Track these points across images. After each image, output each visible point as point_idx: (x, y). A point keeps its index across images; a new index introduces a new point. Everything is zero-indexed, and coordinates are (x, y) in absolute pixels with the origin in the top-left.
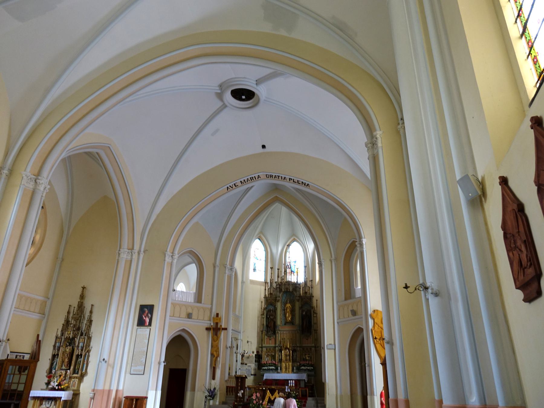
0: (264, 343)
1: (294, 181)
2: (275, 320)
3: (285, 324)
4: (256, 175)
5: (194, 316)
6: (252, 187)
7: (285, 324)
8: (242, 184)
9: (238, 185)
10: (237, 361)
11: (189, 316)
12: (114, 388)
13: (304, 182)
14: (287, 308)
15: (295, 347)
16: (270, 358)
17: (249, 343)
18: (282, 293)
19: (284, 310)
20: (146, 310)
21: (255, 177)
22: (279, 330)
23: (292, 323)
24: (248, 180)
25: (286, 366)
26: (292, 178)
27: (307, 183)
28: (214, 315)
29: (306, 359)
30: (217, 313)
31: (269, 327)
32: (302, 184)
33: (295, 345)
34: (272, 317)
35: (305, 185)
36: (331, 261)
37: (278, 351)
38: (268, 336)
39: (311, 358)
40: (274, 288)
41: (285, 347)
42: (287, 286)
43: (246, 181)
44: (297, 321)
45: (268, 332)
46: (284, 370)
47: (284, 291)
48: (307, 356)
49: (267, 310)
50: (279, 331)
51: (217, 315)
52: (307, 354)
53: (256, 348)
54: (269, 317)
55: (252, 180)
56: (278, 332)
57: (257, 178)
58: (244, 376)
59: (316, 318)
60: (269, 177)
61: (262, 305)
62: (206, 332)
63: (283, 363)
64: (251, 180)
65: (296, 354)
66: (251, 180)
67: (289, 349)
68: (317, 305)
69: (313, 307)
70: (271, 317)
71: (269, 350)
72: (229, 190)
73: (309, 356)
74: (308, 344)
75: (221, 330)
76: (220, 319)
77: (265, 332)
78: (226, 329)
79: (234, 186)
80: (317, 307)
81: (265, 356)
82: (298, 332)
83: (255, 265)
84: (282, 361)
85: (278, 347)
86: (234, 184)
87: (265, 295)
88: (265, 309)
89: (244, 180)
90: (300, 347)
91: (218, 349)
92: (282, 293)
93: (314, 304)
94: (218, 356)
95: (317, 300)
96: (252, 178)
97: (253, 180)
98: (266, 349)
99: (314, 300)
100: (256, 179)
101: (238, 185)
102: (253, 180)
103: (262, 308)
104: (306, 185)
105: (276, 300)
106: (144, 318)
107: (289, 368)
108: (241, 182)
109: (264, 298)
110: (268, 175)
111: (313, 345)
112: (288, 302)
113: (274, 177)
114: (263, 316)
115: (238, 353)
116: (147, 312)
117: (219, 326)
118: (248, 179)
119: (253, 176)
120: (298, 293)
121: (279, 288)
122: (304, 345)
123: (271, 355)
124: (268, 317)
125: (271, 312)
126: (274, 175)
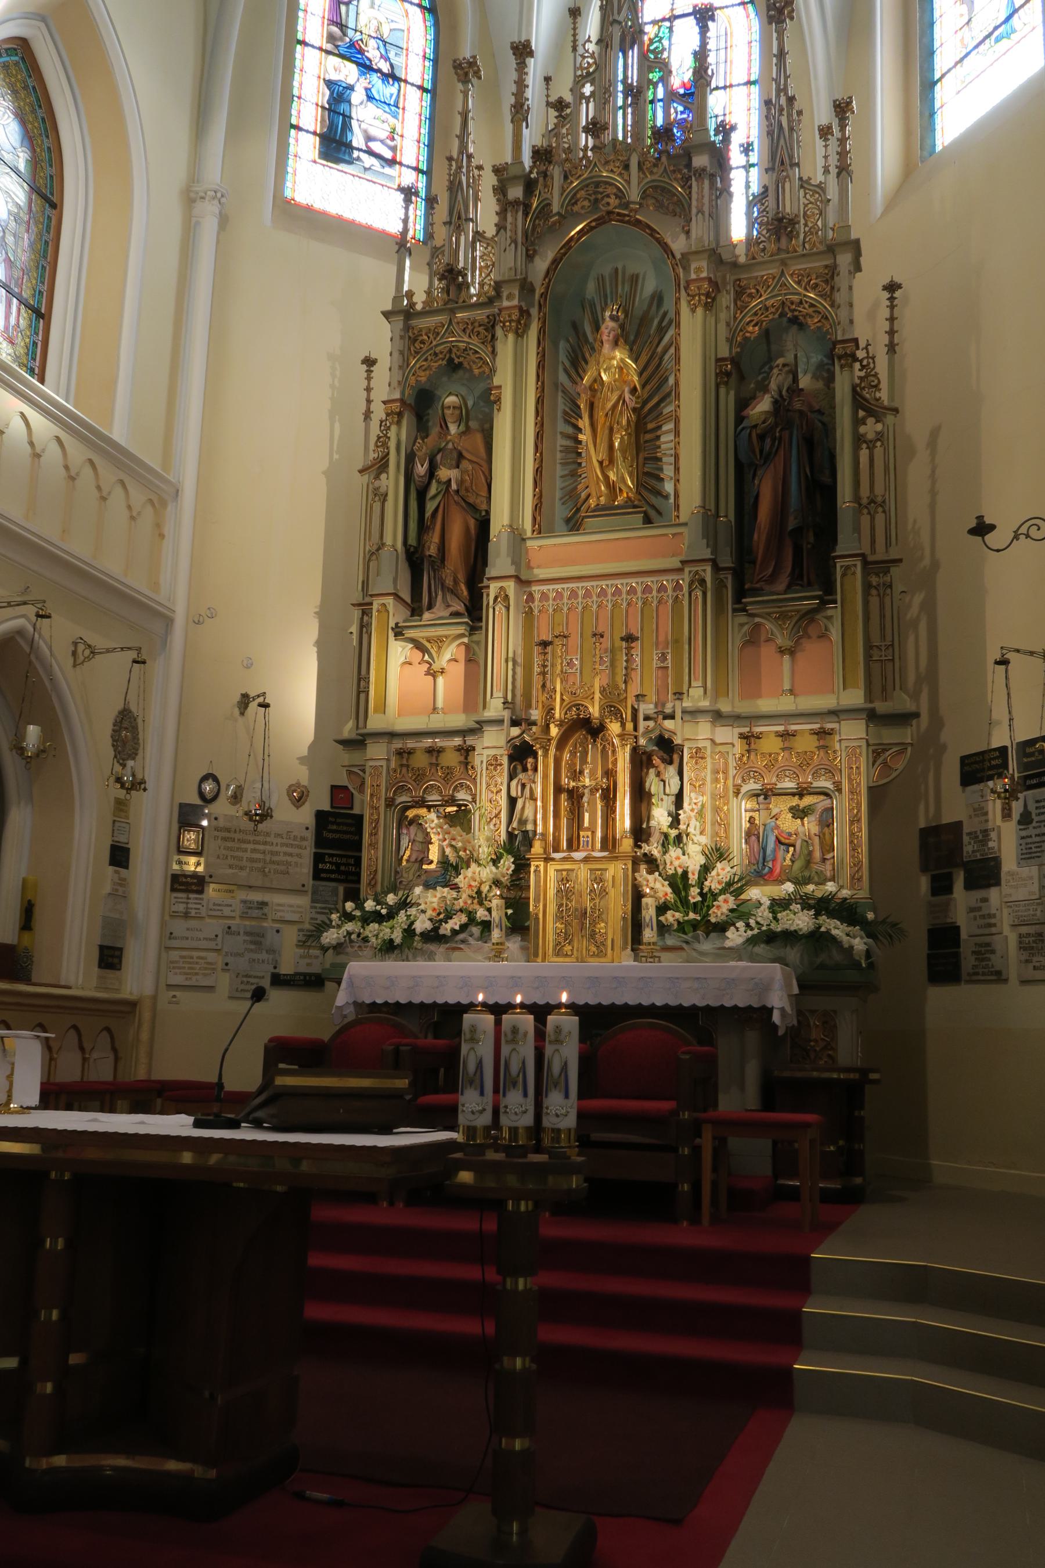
10: (119, 856)
17: (253, 706)
38: (418, 646)
54: (432, 472)
65: (674, 786)
80: (892, 348)
83: (343, 107)
95: (892, 287)
103: (367, 415)
109: (387, 315)
120: (699, 228)
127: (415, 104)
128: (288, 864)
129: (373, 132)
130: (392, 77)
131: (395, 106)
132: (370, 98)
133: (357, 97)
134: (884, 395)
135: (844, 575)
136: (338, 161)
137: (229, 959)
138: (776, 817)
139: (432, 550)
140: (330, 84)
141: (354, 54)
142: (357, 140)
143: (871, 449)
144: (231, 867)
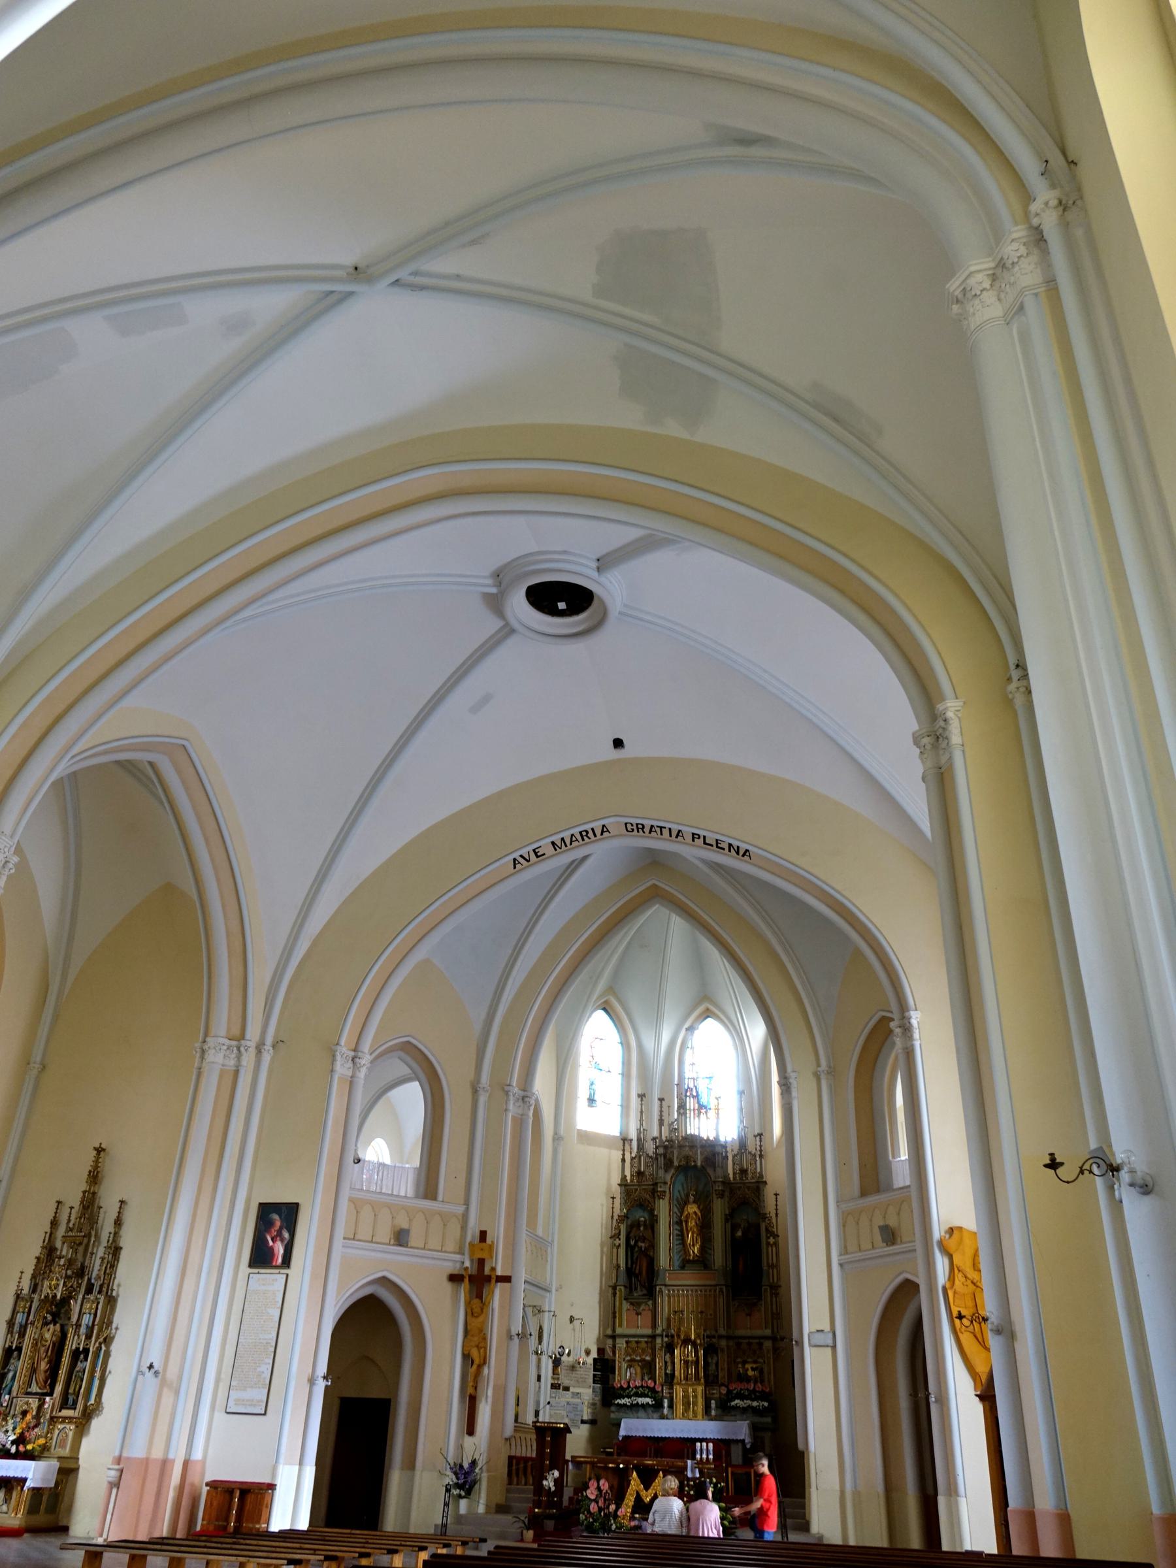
0: (620, 1325)
1: (705, 843)
2: (651, 1254)
3: (682, 1267)
4: (597, 826)
5: (415, 1239)
6: (585, 858)
7: (682, 1267)
8: (556, 850)
9: (544, 854)
10: (539, 1378)
11: (401, 1238)
12: (178, 1456)
13: (735, 843)
14: (688, 1216)
15: (714, 1337)
16: (639, 1369)
17: (577, 1323)
18: (672, 1171)
19: (680, 1223)
20: (276, 1217)
21: (593, 829)
22: (666, 1285)
23: (703, 1262)
24: (574, 839)
25: (686, 1397)
26: (702, 833)
27: (744, 847)
28: (473, 1236)
29: (747, 1374)
30: (483, 1229)
31: (636, 1276)
32: (730, 851)
33: (713, 1333)
34: (643, 1245)
35: (738, 853)
36: (817, 1076)
37: (661, 1349)
38: (632, 1304)
39: (761, 1372)
40: (647, 1155)
41: (682, 1337)
42: (687, 1151)
43: (568, 842)
44: (719, 1257)
45: (631, 1291)
46: (680, 1408)
47: (680, 1166)
48: (748, 1366)
49: (629, 1222)
50: (663, 1288)
51: (483, 1235)
52: (749, 1360)
53: (595, 1340)
54: (636, 1243)
55: (585, 838)
56: (661, 1291)
57: (598, 832)
58: (562, 1426)
59: (774, 1249)
60: (633, 830)
61: (613, 1208)
62: (448, 1286)
63: (678, 1387)
64: (583, 840)
65: (715, 1358)
66: (583, 840)
67: (694, 1344)
68: (777, 1210)
69: (764, 1217)
70: (640, 1244)
71: (634, 1345)
72: (518, 866)
73: (754, 1366)
74: (750, 1328)
75: (493, 1281)
76: (491, 1247)
77: (623, 1288)
78: (507, 1279)
79: (532, 854)
80: (777, 1215)
81: (624, 1365)
82: (721, 1291)
83: (593, 1087)
84: (675, 1381)
85: (662, 1336)
86: (534, 850)
87: (624, 1178)
88: (622, 1219)
89: (563, 839)
90: (728, 1338)
91: (485, 1339)
92: (672, 1171)
93: (770, 1206)
94: (484, 1361)
95: (776, 1195)
96: (584, 834)
97: (589, 838)
98: (627, 1342)
99: (769, 1192)
100: (595, 836)
101: (544, 854)
102: (589, 838)
103: (612, 1217)
104: (741, 853)
105: (655, 1193)
106: (271, 1243)
107: (695, 1404)
108: (553, 843)
110: (632, 825)
111: (768, 1332)
112: (692, 1198)
113: (647, 830)
114: (617, 1242)
115: (541, 1352)
116: (278, 1224)
117: (487, 1271)
118: (572, 835)
119: (588, 827)
120: (719, 1171)
121: (665, 1155)
122: (741, 1332)
123: (643, 1360)
124: (632, 1243)
125: (642, 1228)
126: (647, 823)
128: (586, 1378)
134: (775, 1230)
135: (765, 1291)
136: (592, 1107)
138: (748, 1369)
139: (637, 1271)
142: (596, 1098)
143: (772, 1247)
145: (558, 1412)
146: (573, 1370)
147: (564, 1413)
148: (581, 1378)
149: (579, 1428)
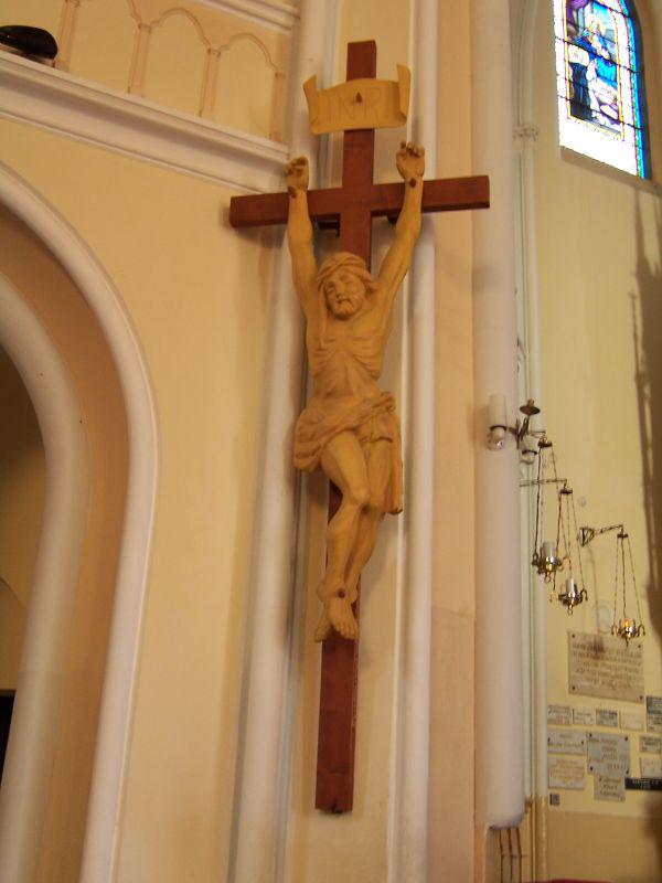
30: (360, 36)
51: (362, 59)
62: (230, 248)
76: (396, 91)
78: (469, 194)
91: (387, 404)
94: (387, 507)
115: (557, 563)
117: (386, 174)
127: (625, 78)
129: (603, 99)
130: (611, 62)
131: (613, 82)
132: (598, 75)
133: (590, 74)
137: (593, 764)
140: (572, 65)
141: (584, 44)
142: (594, 105)
144: (588, 679)
145: (568, 758)
146: (596, 657)
147: (583, 761)
148: (617, 676)
149: (623, 799)
